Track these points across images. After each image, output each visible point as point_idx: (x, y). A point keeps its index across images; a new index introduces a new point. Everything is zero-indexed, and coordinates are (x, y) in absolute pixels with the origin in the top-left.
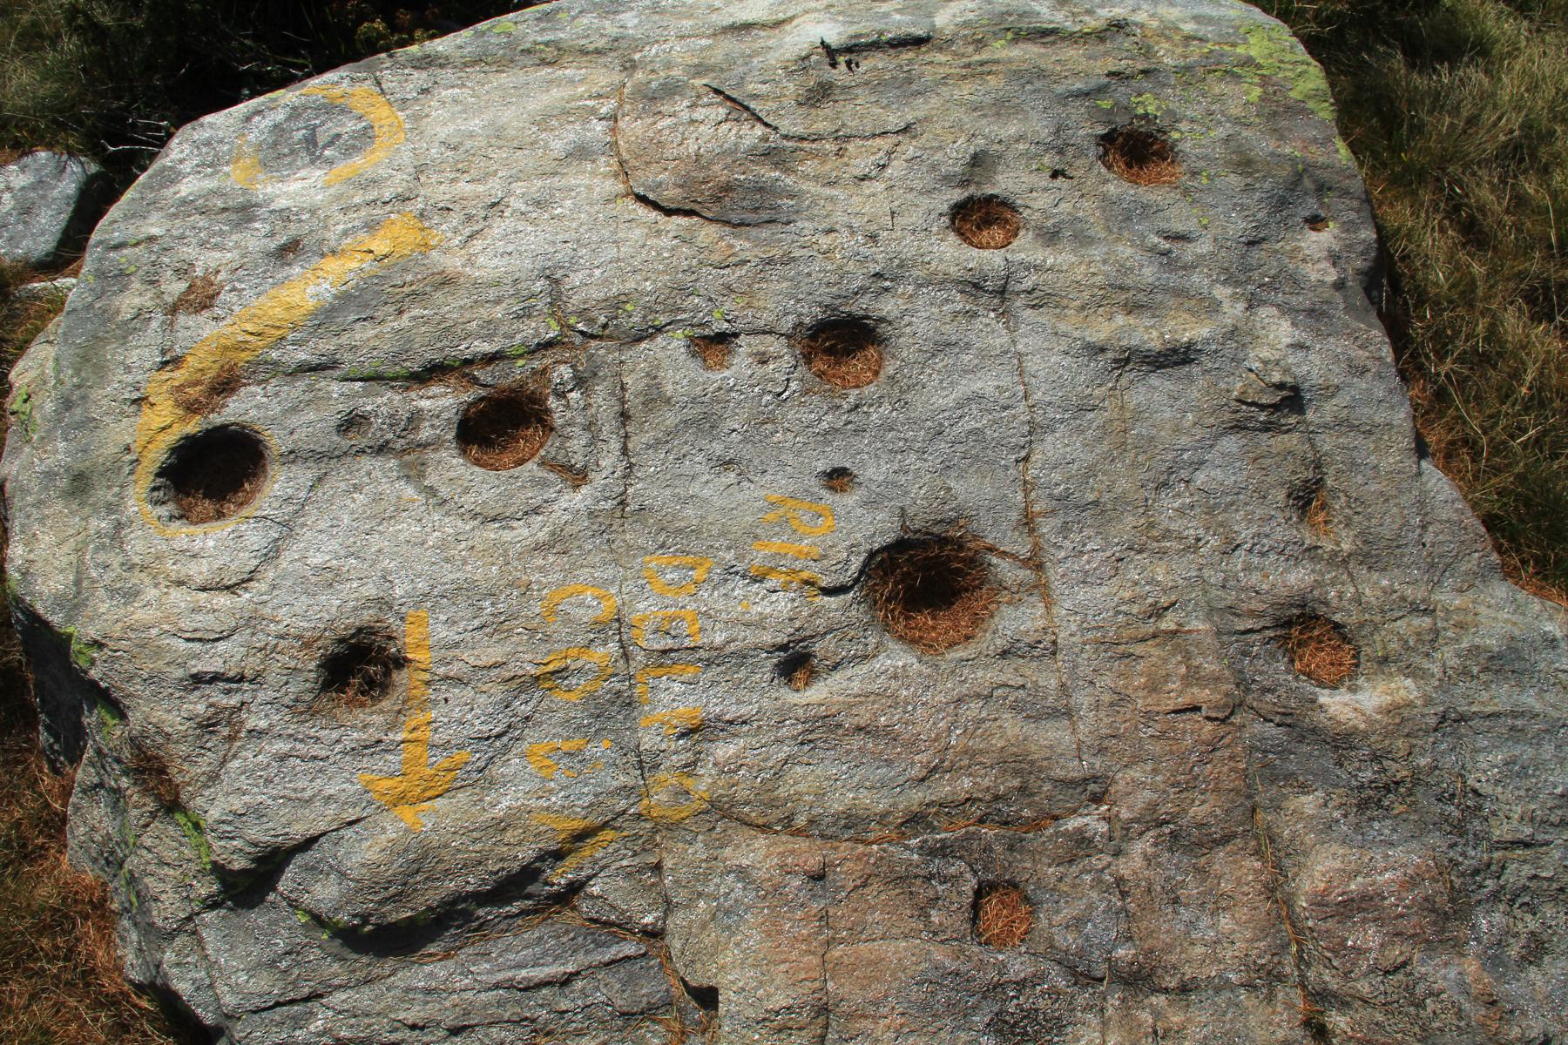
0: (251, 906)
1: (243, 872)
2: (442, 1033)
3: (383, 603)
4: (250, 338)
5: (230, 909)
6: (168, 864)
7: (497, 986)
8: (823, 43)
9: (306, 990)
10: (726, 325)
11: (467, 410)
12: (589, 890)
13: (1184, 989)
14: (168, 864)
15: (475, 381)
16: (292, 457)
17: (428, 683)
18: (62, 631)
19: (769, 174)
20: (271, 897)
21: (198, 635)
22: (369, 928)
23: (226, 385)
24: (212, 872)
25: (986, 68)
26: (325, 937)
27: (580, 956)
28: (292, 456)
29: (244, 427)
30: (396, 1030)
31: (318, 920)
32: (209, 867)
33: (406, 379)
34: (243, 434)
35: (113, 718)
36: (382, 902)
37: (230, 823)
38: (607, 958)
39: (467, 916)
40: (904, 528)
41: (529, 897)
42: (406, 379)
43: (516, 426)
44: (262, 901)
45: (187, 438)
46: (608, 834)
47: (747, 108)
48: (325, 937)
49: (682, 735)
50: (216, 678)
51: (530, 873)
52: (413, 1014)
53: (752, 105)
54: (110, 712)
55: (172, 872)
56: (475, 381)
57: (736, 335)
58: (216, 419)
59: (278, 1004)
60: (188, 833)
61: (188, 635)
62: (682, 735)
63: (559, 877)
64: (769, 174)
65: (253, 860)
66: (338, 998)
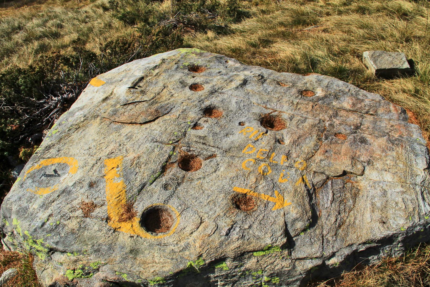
0: (294, 245)
1: (287, 240)
2: (339, 216)
3: (227, 193)
4: (119, 198)
5: (293, 250)
6: (274, 261)
7: (331, 204)
8: (129, 88)
9: (321, 238)
10: (193, 123)
11: (180, 167)
12: (315, 184)
13: (361, 124)
14: (274, 261)
15: (173, 163)
16: (166, 202)
17: (254, 192)
18: (188, 266)
19: (155, 106)
20: (294, 239)
21: (214, 231)
22: (311, 220)
23: (129, 208)
24: (282, 250)
25: (159, 74)
26: (309, 231)
27: (329, 190)
28: (166, 201)
29: (147, 209)
30: (336, 224)
31: (304, 230)
32: (281, 250)
33: (161, 174)
34: (149, 210)
35: (223, 263)
36: (306, 215)
37: (273, 238)
38: (331, 186)
39: (313, 204)
40: (259, 120)
41: (312, 194)
42: (161, 174)
43: (189, 163)
44: (294, 242)
45: (140, 222)
46: (304, 177)
47: (136, 102)
48: (309, 231)
49: (288, 159)
50: (229, 230)
51: (308, 190)
52: (333, 219)
53: (136, 101)
54: (219, 264)
55: (277, 261)
56: (173, 163)
57: (197, 123)
58: (140, 213)
59: (323, 244)
60: (268, 253)
61: (212, 233)
62: (288, 159)
63: (310, 187)
64: (155, 106)
65: (285, 237)
66: (325, 232)
